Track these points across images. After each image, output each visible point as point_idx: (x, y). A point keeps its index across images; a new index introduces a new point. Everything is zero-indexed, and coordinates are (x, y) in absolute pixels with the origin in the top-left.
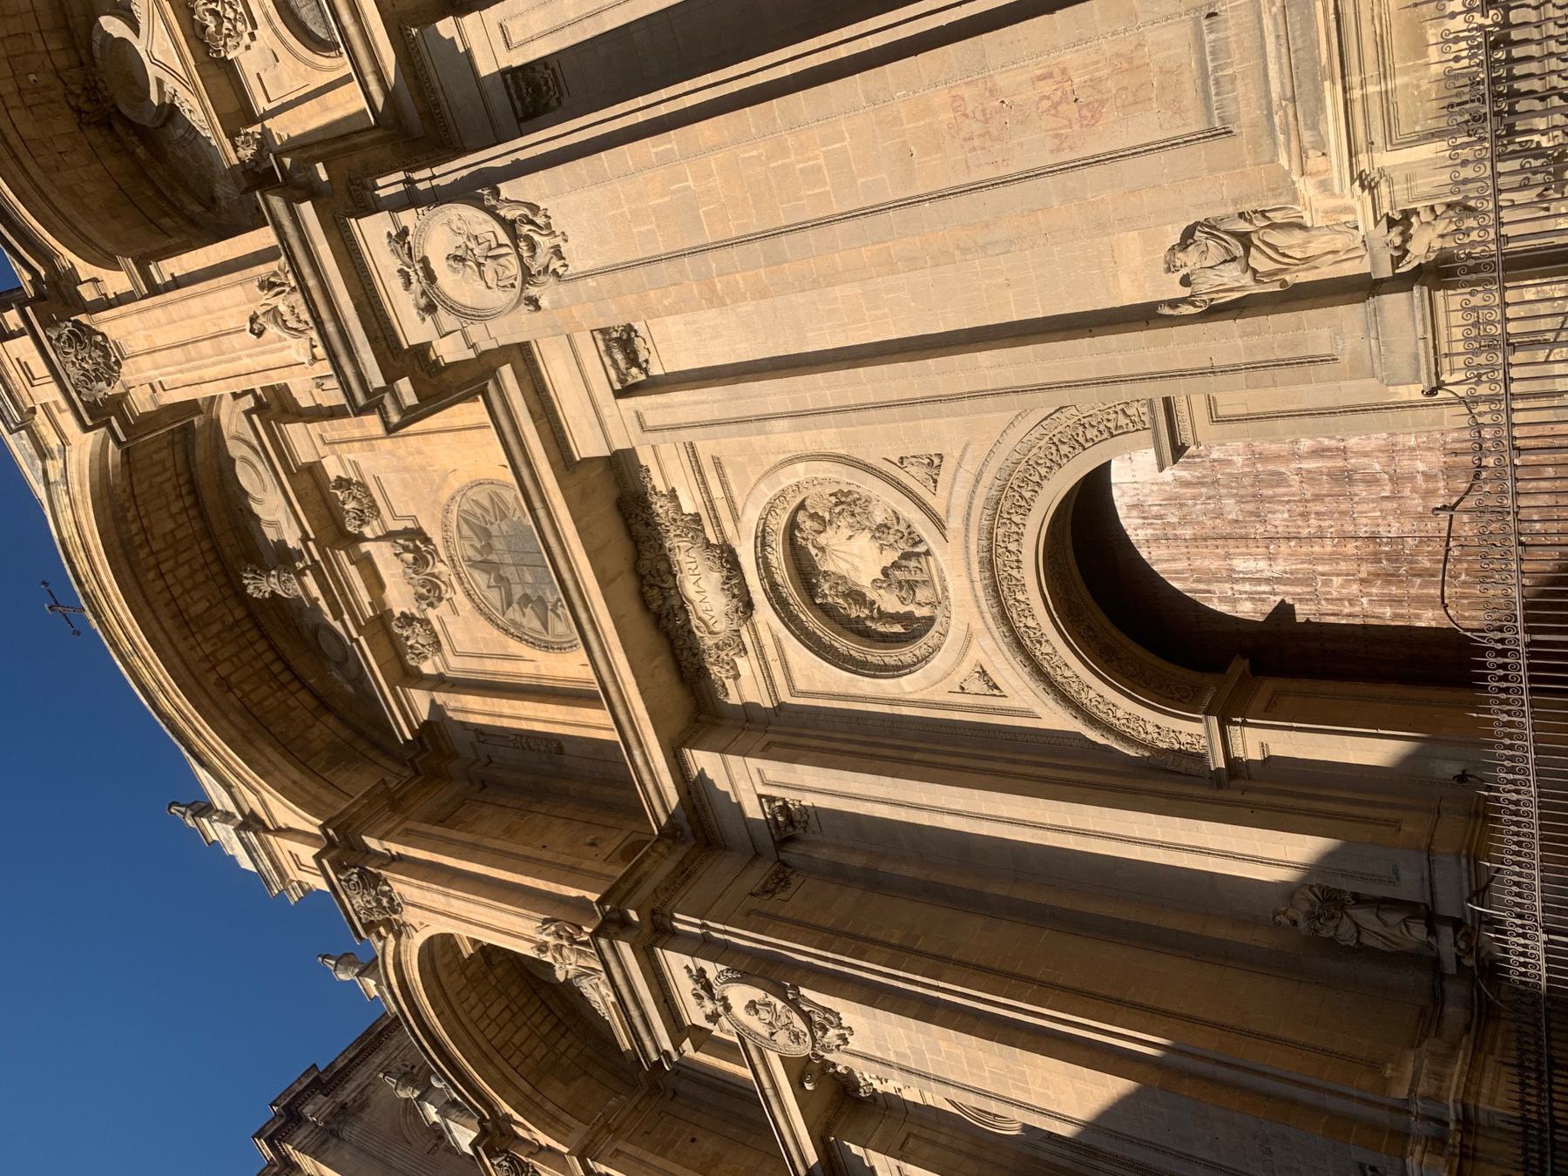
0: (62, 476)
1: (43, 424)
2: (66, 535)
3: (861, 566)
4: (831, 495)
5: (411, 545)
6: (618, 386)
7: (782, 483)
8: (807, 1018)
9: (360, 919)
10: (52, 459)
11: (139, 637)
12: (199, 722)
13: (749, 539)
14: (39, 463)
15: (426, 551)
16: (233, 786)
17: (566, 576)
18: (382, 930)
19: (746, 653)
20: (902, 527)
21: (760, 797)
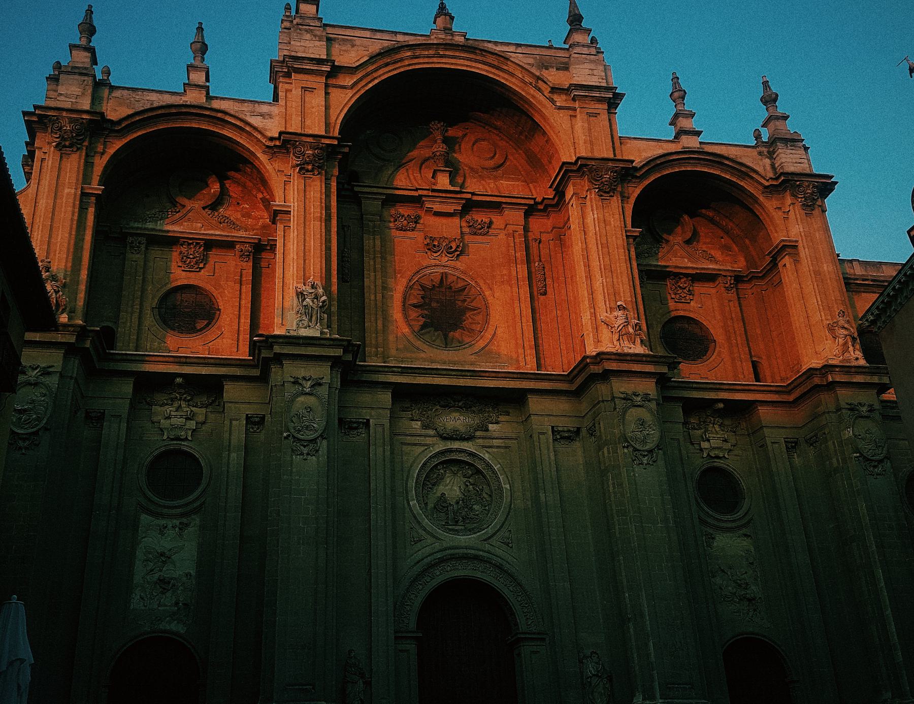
0: (540, 88)
1: (566, 100)
2: (509, 63)
3: (447, 488)
4: (483, 487)
5: (458, 249)
6: (555, 428)
7: (501, 475)
8: (313, 441)
9: (295, 141)
10: (550, 91)
11: (446, 63)
12: (393, 70)
13: (476, 450)
14: (551, 85)
15: (454, 256)
16: (356, 71)
17: (487, 374)
18: (278, 143)
19: (424, 429)
20: (471, 515)
21: (368, 420)
